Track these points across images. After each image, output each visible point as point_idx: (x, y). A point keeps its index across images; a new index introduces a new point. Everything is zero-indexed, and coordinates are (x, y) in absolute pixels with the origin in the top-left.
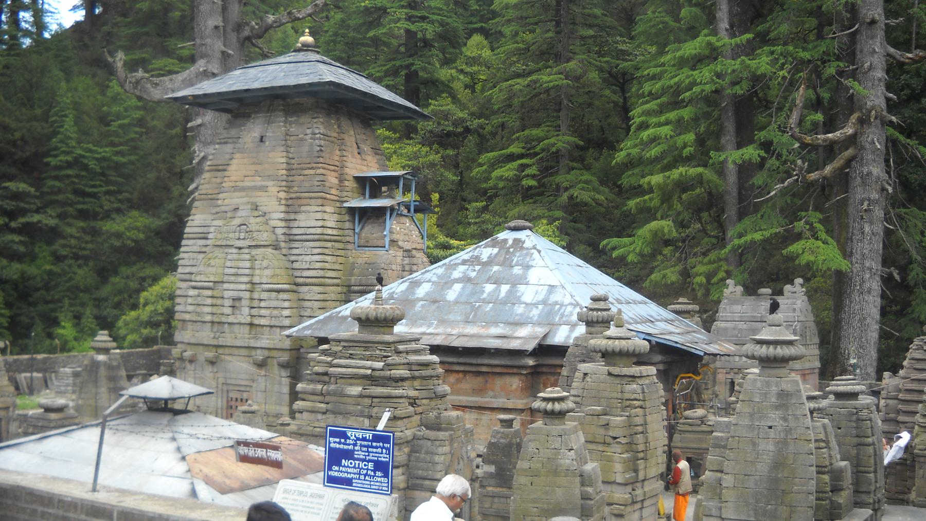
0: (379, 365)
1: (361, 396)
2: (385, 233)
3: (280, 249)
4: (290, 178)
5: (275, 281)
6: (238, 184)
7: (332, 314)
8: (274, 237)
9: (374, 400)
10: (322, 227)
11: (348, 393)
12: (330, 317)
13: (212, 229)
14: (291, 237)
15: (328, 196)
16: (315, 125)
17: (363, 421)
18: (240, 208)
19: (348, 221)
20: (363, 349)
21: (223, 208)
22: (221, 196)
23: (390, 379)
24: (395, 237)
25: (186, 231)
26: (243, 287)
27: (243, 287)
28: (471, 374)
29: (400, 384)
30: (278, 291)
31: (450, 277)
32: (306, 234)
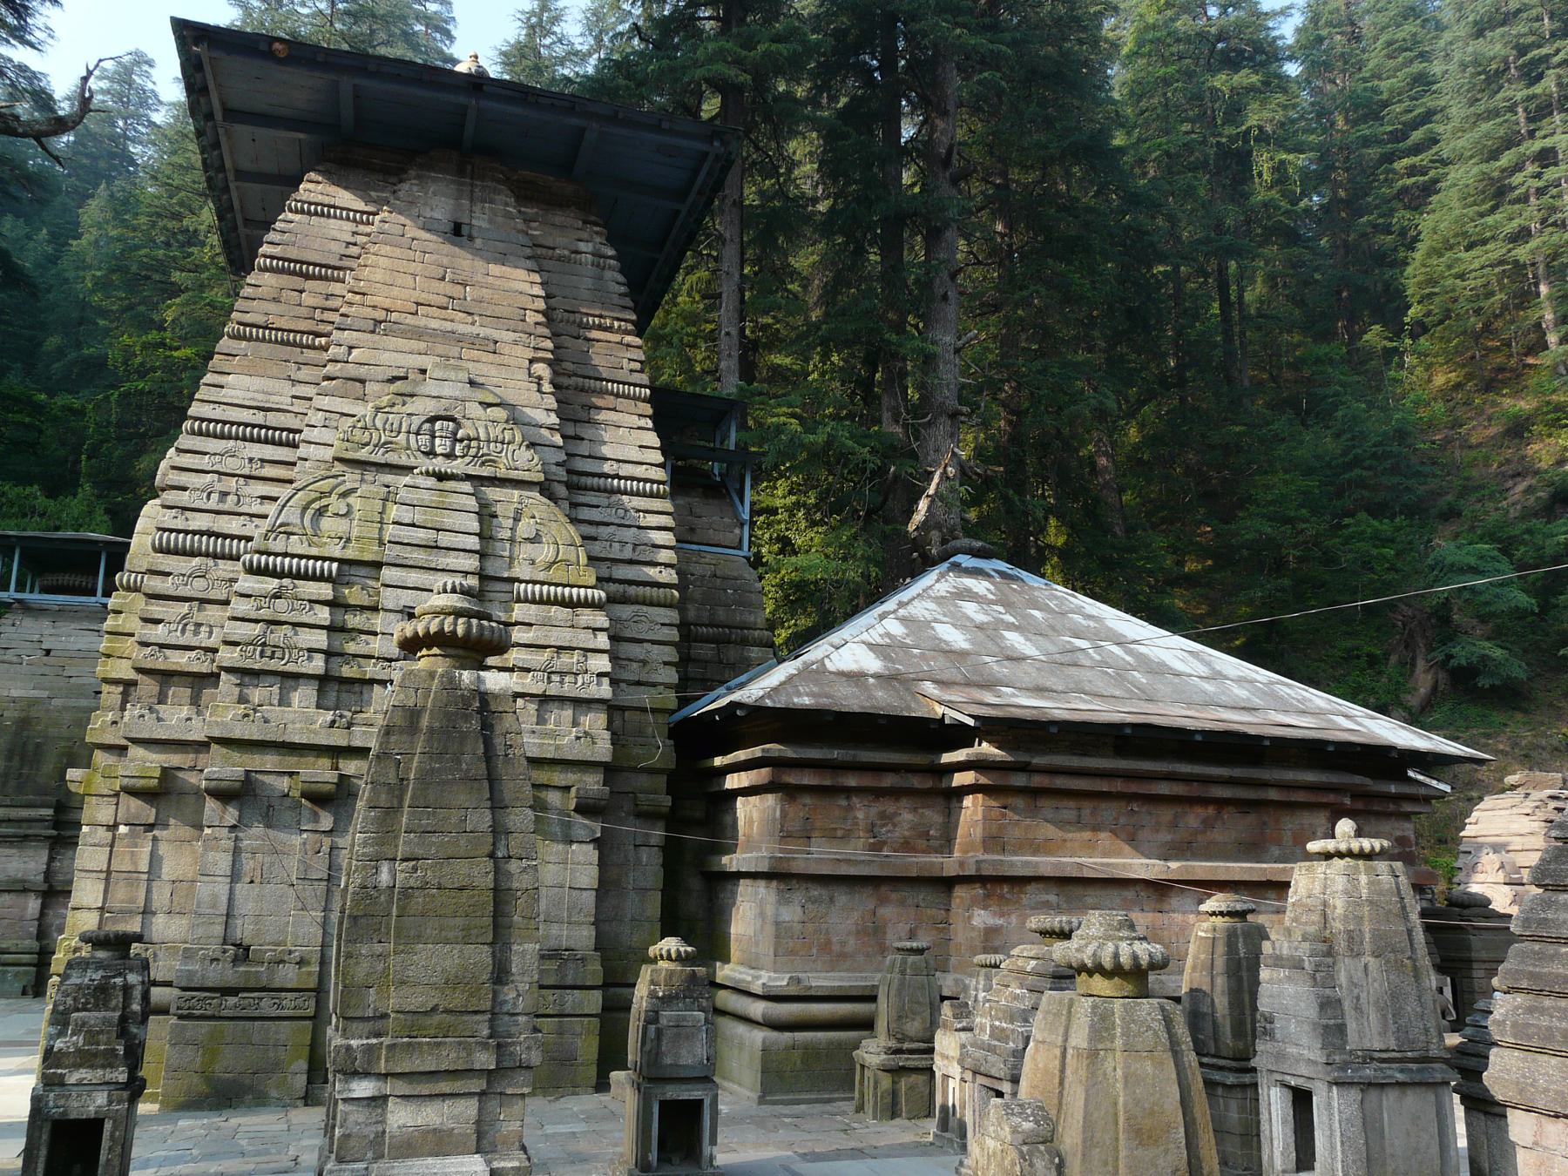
25: (190, 412)
28: (1231, 809)
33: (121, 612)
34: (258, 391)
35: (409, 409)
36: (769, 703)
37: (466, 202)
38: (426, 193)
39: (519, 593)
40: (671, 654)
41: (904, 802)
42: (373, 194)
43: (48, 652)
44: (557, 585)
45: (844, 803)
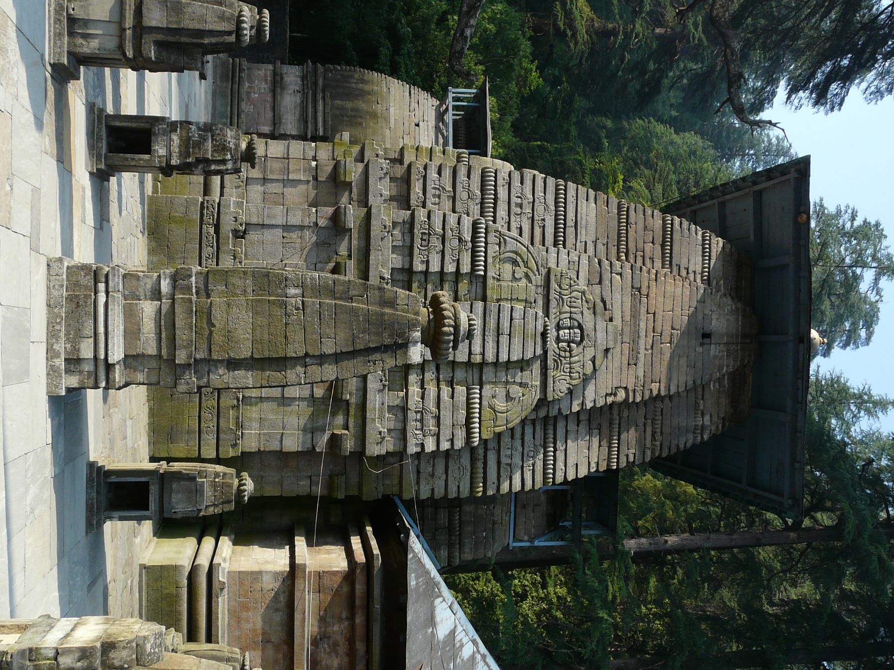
5: (487, 412)
33: (444, 154)
34: (587, 221)
35: (586, 312)
36: (410, 556)
37: (725, 340)
38: (727, 315)
39: (473, 389)
40: (439, 493)
41: (346, 659)
42: (722, 282)
43: (417, 125)
44: (480, 413)
45: (344, 615)
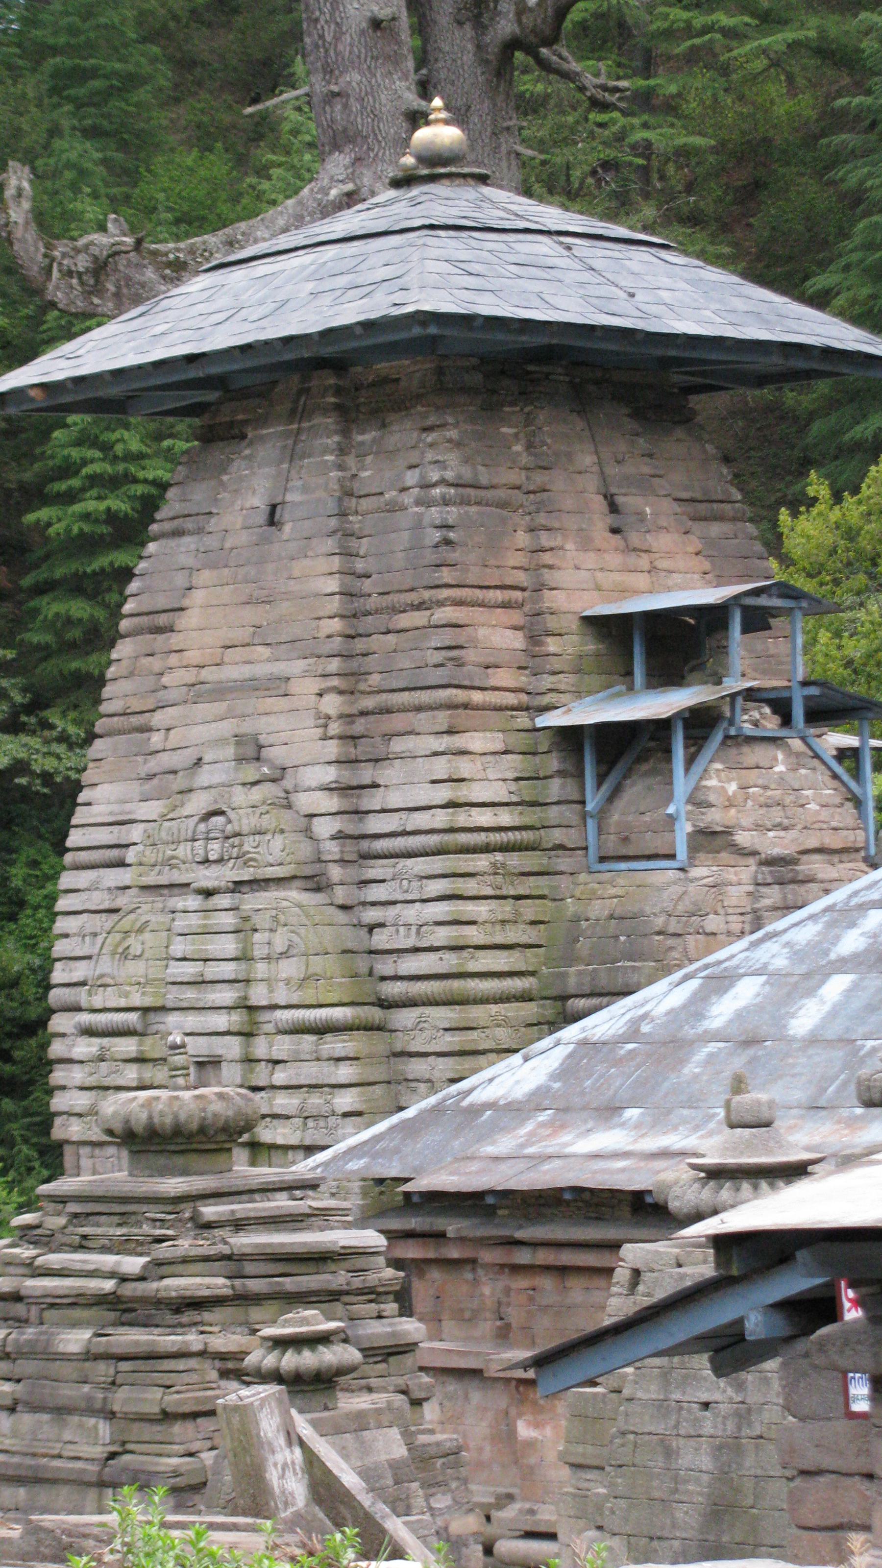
0: (133, 1264)
1: (90, 1356)
2: (671, 810)
3: (330, 886)
4: (360, 645)
5: (309, 995)
6: (206, 674)
7: (444, 1100)
8: (305, 849)
9: (124, 1366)
10: (452, 805)
11: (61, 1348)
12: (437, 1110)
13: (136, 833)
14: (365, 845)
15: (477, 697)
16: (430, 456)
17: (95, 1427)
18: (207, 758)
19: (561, 773)
20: (116, 1219)
21: (166, 760)
22: (158, 719)
23: (158, 1303)
24: (715, 818)
26: (221, 1021)
27: (221, 1021)
29: (186, 1317)
30: (321, 1030)
31: (826, 953)
32: (405, 833)
45: (469, 1276)
